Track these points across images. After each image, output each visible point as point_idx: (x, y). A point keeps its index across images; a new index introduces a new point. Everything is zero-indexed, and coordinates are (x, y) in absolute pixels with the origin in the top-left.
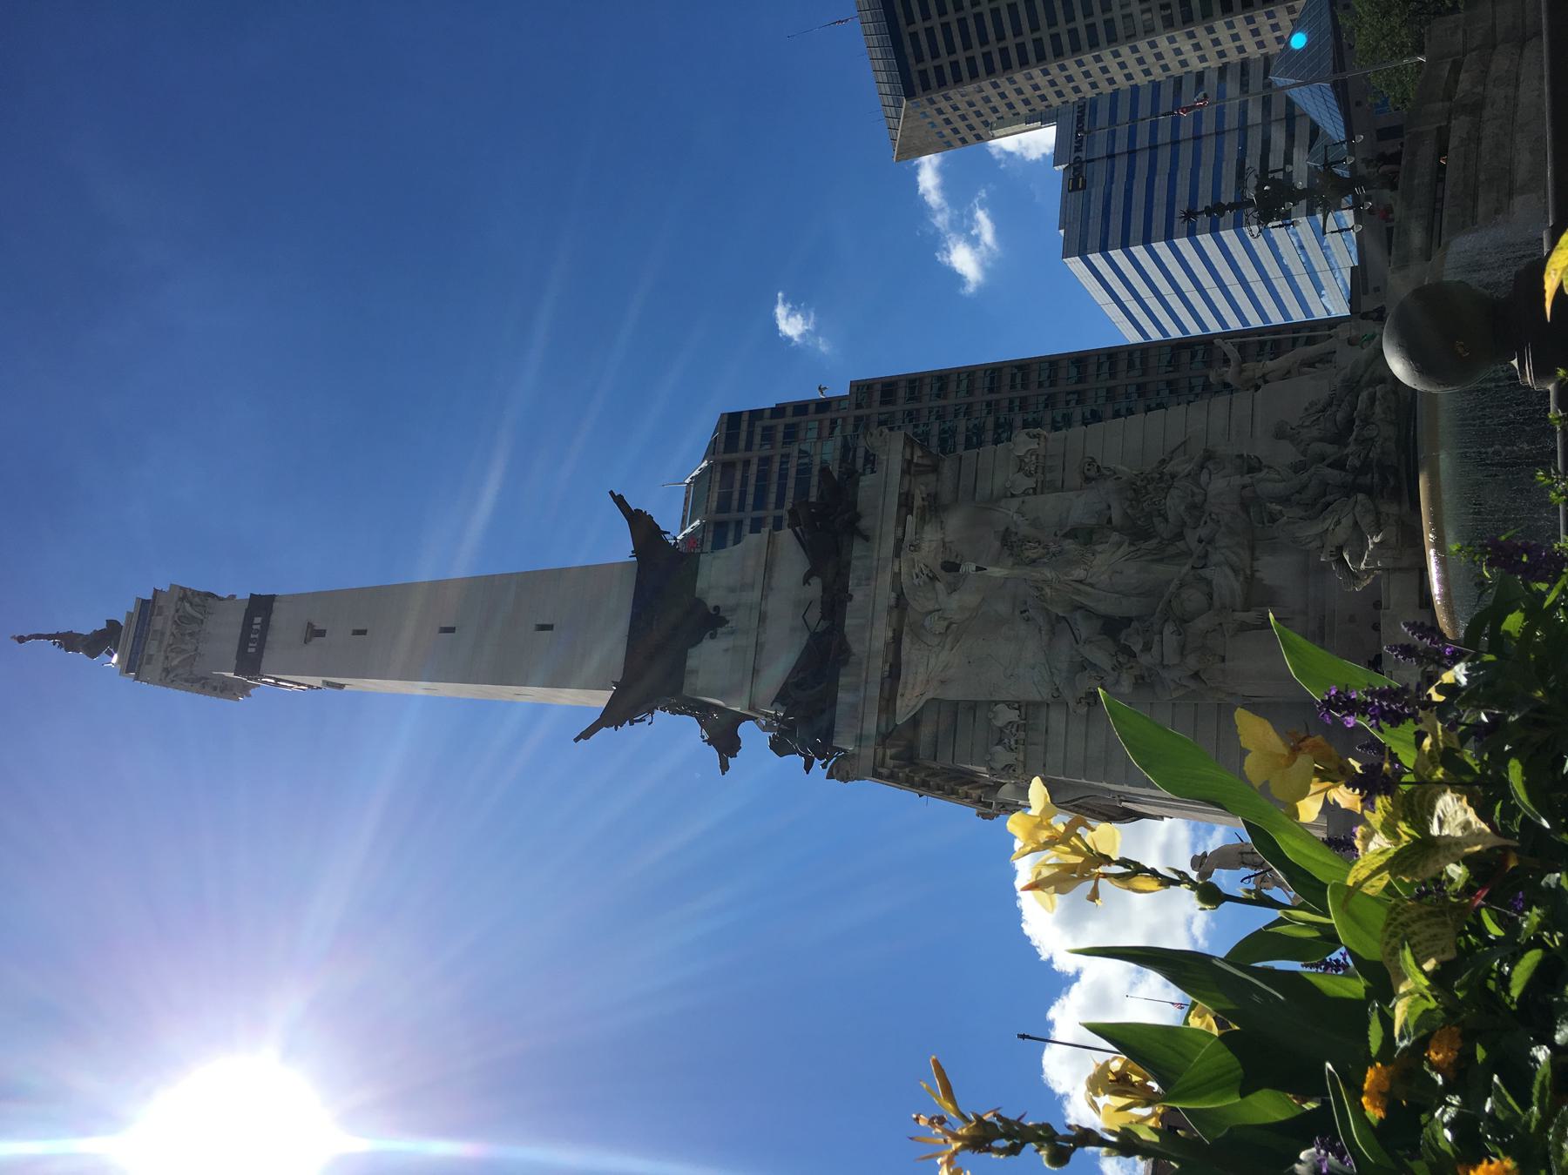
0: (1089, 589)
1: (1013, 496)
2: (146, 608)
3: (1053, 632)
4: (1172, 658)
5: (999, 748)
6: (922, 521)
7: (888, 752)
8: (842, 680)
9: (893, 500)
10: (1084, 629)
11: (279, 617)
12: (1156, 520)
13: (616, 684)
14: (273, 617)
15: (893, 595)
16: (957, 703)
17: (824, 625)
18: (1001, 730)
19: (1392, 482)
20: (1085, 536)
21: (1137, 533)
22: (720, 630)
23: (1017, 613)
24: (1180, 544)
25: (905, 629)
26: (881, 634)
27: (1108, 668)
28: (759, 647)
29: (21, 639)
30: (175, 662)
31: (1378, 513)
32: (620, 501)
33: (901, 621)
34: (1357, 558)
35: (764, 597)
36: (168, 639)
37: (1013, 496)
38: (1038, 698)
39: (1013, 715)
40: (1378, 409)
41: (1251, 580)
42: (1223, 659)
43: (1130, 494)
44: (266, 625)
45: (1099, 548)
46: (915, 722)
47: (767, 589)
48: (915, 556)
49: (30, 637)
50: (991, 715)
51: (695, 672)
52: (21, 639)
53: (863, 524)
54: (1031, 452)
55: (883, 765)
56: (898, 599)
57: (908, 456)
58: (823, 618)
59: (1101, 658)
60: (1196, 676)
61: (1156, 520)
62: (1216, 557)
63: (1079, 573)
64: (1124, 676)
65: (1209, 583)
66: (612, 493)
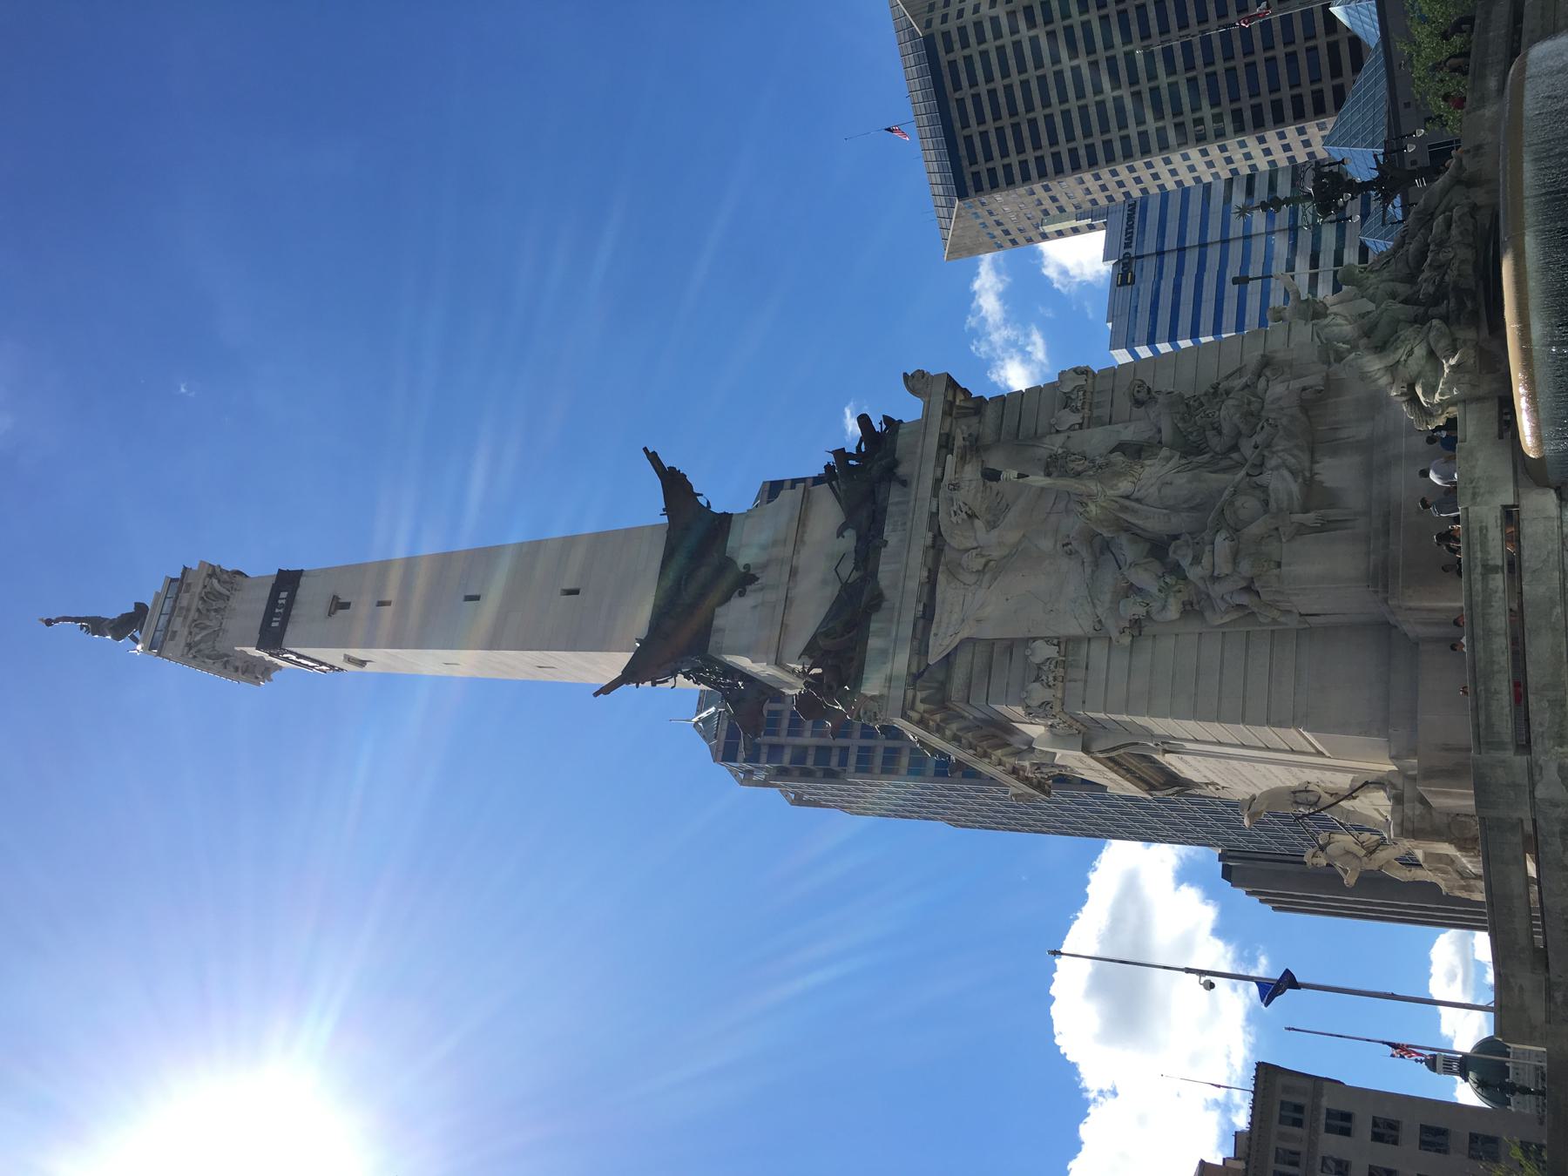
0: (1136, 505)
2: (178, 585)
3: (1096, 564)
4: (1224, 568)
5: (1037, 685)
6: (963, 459)
7: (920, 695)
8: (874, 626)
9: (933, 441)
10: (1129, 551)
11: (304, 591)
12: (1210, 434)
13: (639, 641)
14: (299, 591)
15: (930, 534)
16: (992, 643)
17: (856, 575)
18: (1039, 667)
19: (1469, 305)
20: (1135, 451)
21: (1190, 448)
22: (749, 588)
23: (1059, 546)
24: (1235, 456)
25: (941, 568)
26: (918, 574)
27: (1154, 590)
28: (788, 600)
29: (49, 622)
30: (198, 638)
31: (1455, 340)
32: (653, 458)
33: (937, 561)
34: (1430, 390)
35: (795, 551)
36: (193, 614)
38: (1078, 632)
39: (1052, 651)
40: (1454, 231)
41: (1310, 484)
42: (1279, 565)
43: (1182, 408)
44: (291, 600)
45: (1148, 462)
46: (948, 660)
47: (799, 542)
48: (956, 495)
49: (57, 621)
50: (1028, 652)
51: (722, 630)
52: (49, 622)
53: (902, 470)
54: (1079, 388)
55: (912, 708)
56: (935, 537)
57: (950, 398)
58: (856, 568)
59: (1145, 578)
60: (1249, 589)
61: (1210, 434)
62: (1273, 462)
63: (1125, 486)
64: (1171, 600)
65: (1264, 488)
66: (645, 449)
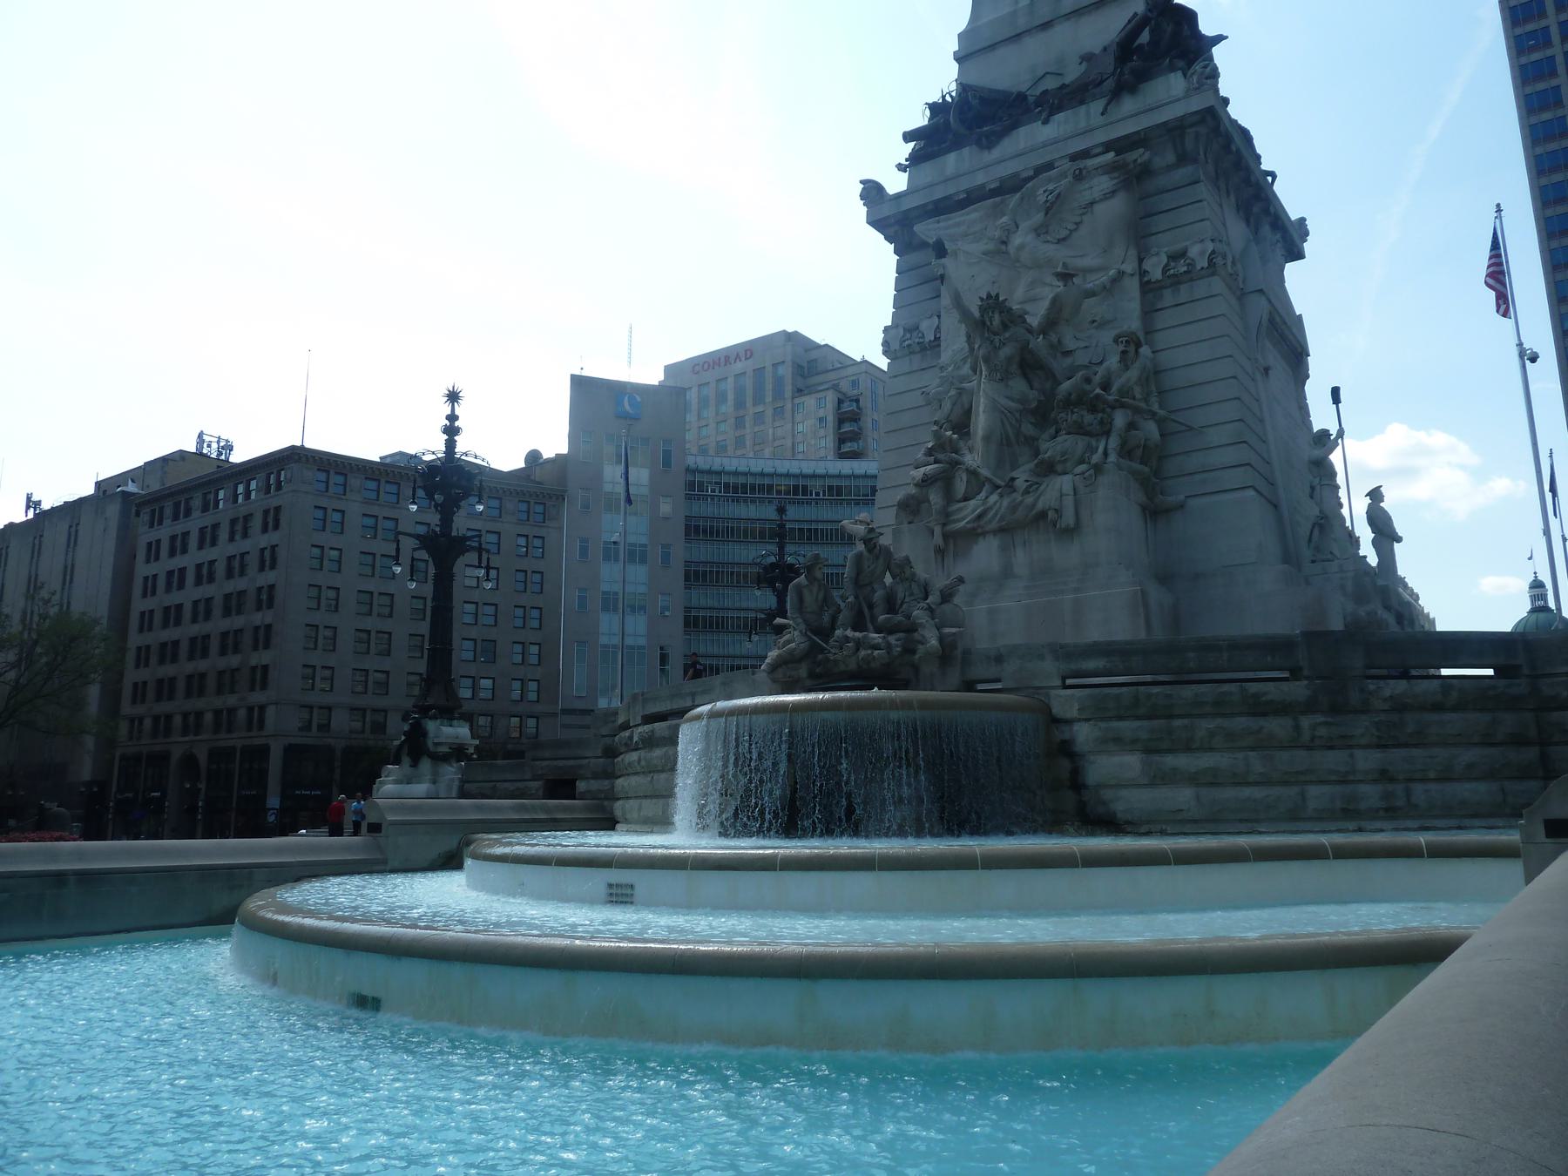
1: (1141, 260)
8: (966, 151)
15: (1031, 173)
25: (998, 199)
35: (1068, 16)
37: (1141, 260)
54: (1191, 265)
61: (1052, 430)
